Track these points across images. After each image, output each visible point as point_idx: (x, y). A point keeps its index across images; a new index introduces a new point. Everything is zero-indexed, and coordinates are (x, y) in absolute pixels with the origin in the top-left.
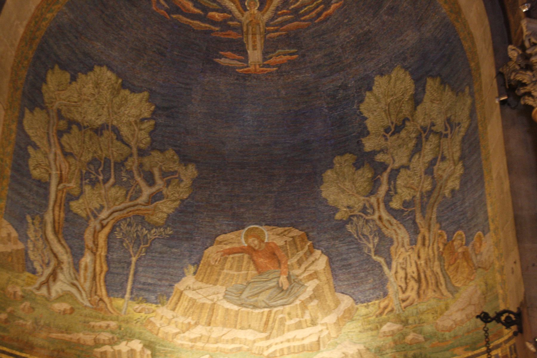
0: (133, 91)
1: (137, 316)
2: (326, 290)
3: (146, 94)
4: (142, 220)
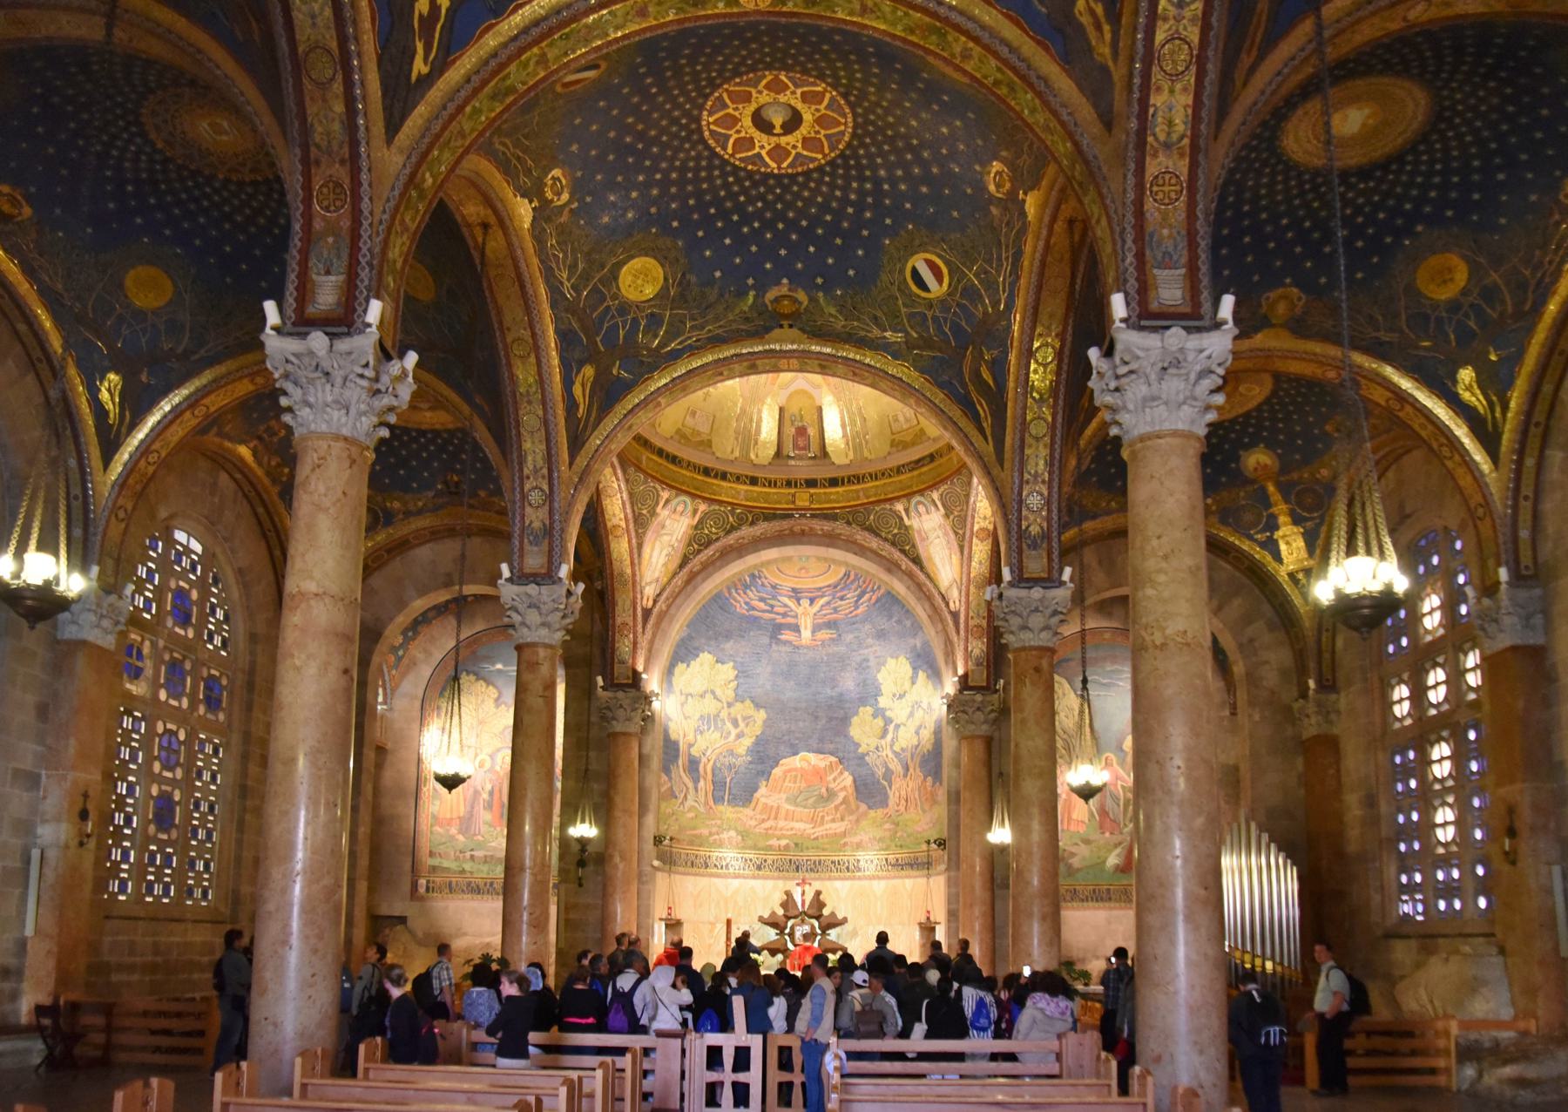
0: (723, 663)
1: (731, 816)
2: (852, 800)
3: (731, 664)
4: (731, 753)
